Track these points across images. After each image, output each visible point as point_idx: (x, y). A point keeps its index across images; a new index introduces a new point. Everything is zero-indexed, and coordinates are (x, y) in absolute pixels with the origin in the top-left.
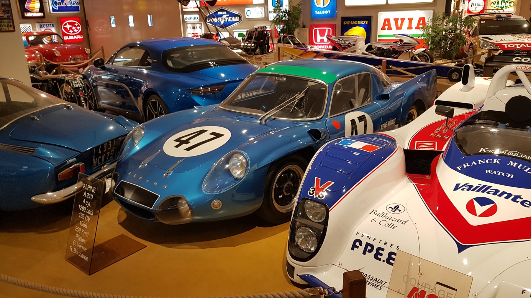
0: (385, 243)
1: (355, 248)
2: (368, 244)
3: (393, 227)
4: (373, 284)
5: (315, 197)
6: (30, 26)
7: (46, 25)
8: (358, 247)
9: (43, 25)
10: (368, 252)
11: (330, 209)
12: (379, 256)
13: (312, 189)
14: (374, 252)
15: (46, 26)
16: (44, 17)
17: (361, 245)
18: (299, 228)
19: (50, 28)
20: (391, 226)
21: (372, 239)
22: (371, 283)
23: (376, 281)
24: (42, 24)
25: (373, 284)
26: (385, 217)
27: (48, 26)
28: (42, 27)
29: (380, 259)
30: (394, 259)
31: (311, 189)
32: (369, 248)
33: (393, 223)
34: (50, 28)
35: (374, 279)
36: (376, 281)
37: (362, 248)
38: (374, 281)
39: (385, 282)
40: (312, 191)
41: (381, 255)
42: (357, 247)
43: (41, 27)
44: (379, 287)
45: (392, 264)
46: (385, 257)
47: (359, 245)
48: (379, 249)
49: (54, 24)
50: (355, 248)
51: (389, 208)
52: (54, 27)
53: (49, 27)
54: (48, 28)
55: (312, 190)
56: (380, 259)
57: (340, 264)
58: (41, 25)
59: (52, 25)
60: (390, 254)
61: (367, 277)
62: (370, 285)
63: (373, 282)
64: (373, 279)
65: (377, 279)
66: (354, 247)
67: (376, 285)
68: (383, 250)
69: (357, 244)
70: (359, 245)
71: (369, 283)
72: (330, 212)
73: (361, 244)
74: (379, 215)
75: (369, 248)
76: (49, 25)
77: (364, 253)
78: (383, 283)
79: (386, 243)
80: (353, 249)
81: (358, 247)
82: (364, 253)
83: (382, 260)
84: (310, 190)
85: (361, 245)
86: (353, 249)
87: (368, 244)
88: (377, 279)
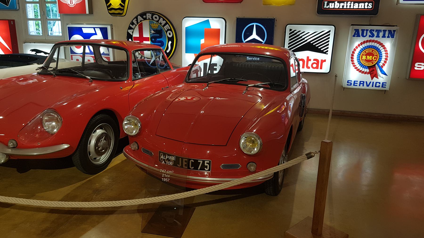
6: (329, 31)
7: (371, 31)
9: (363, 31)
15: (369, 34)
16: (374, 12)
19: (380, 40)
24: (360, 28)
27: (375, 34)
28: (358, 36)
34: (380, 40)
43: (354, 36)
49: (394, 31)
52: (393, 37)
53: (378, 36)
54: (374, 38)
58: (357, 31)
59: (390, 32)
76: (378, 31)
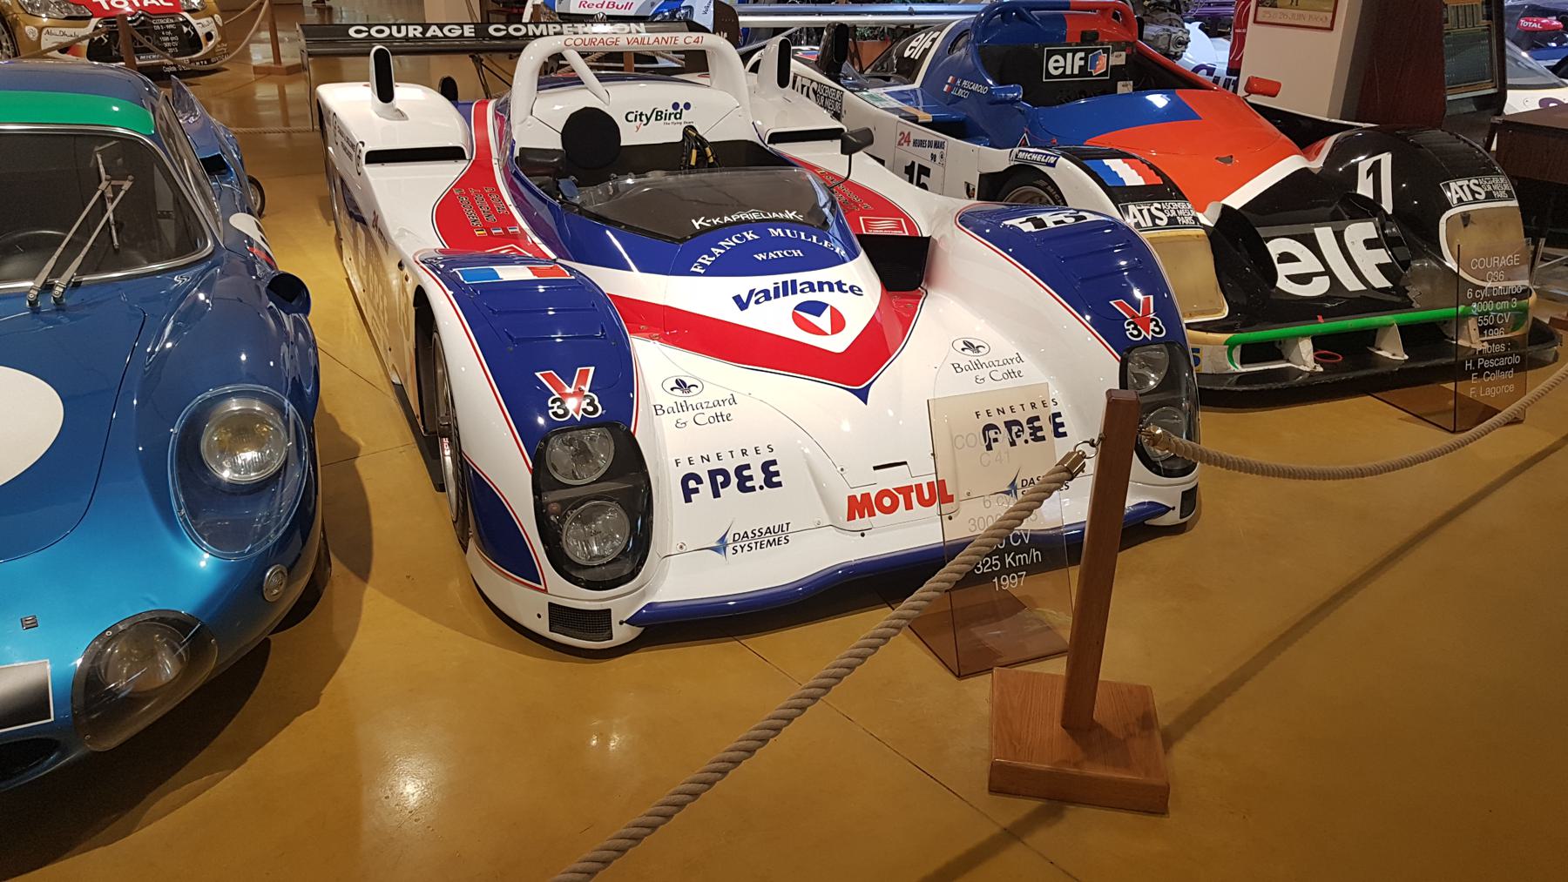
0: (743, 453)
1: (693, 496)
2: (713, 474)
3: (725, 418)
4: (769, 541)
5: (579, 418)
8: (697, 488)
10: (722, 488)
11: (632, 430)
12: (748, 484)
13: (553, 402)
14: (734, 480)
17: (702, 483)
18: (562, 520)
20: (720, 418)
21: (713, 458)
22: (766, 542)
23: (770, 532)
25: (769, 541)
26: (690, 408)
29: (752, 489)
30: (777, 474)
31: (550, 405)
32: (720, 479)
33: (718, 410)
35: (764, 531)
36: (770, 532)
37: (706, 488)
38: (767, 535)
39: (788, 524)
40: (558, 407)
41: (750, 478)
42: (696, 491)
44: (783, 539)
45: (779, 484)
46: (759, 478)
47: (697, 484)
48: (739, 470)
50: (693, 496)
51: (672, 389)
55: (555, 405)
56: (752, 489)
57: (681, 547)
60: (765, 466)
61: (750, 536)
62: (765, 546)
63: (766, 540)
64: (762, 533)
65: (769, 528)
66: (688, 494)
67: (774, 540)
68: (747, 467)
69: (692, 484)
70: (697, 484)
71: (761, 544)
72: (636, 436)
73: (699, 480)
74: (675, 410)
75: (720, 479)
77: (716, 494)
78: (785, 528)
79: (744, 453)
80: (688, 500)
81: (697, 488)
82: (716, 494)
83: (757, 488)
84: (553, 408)
85: (702, 483)
86: (688, 500)
87: (713, 474)
88: (769, 528)
